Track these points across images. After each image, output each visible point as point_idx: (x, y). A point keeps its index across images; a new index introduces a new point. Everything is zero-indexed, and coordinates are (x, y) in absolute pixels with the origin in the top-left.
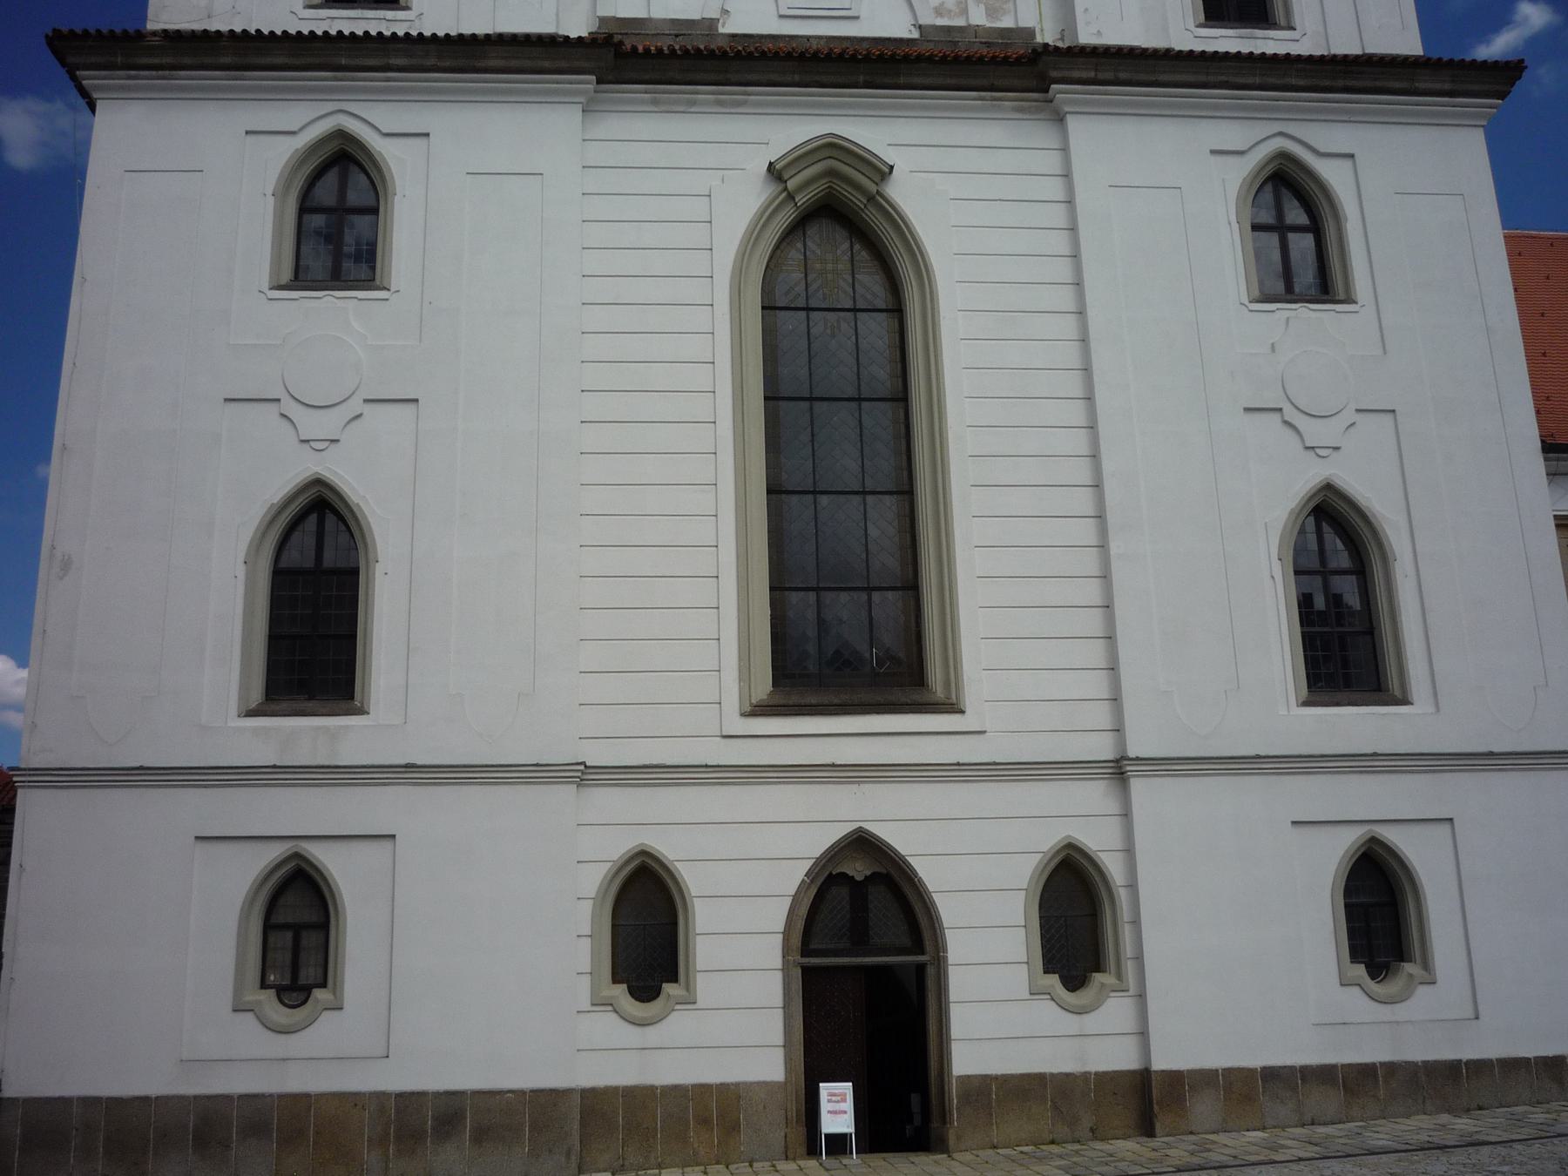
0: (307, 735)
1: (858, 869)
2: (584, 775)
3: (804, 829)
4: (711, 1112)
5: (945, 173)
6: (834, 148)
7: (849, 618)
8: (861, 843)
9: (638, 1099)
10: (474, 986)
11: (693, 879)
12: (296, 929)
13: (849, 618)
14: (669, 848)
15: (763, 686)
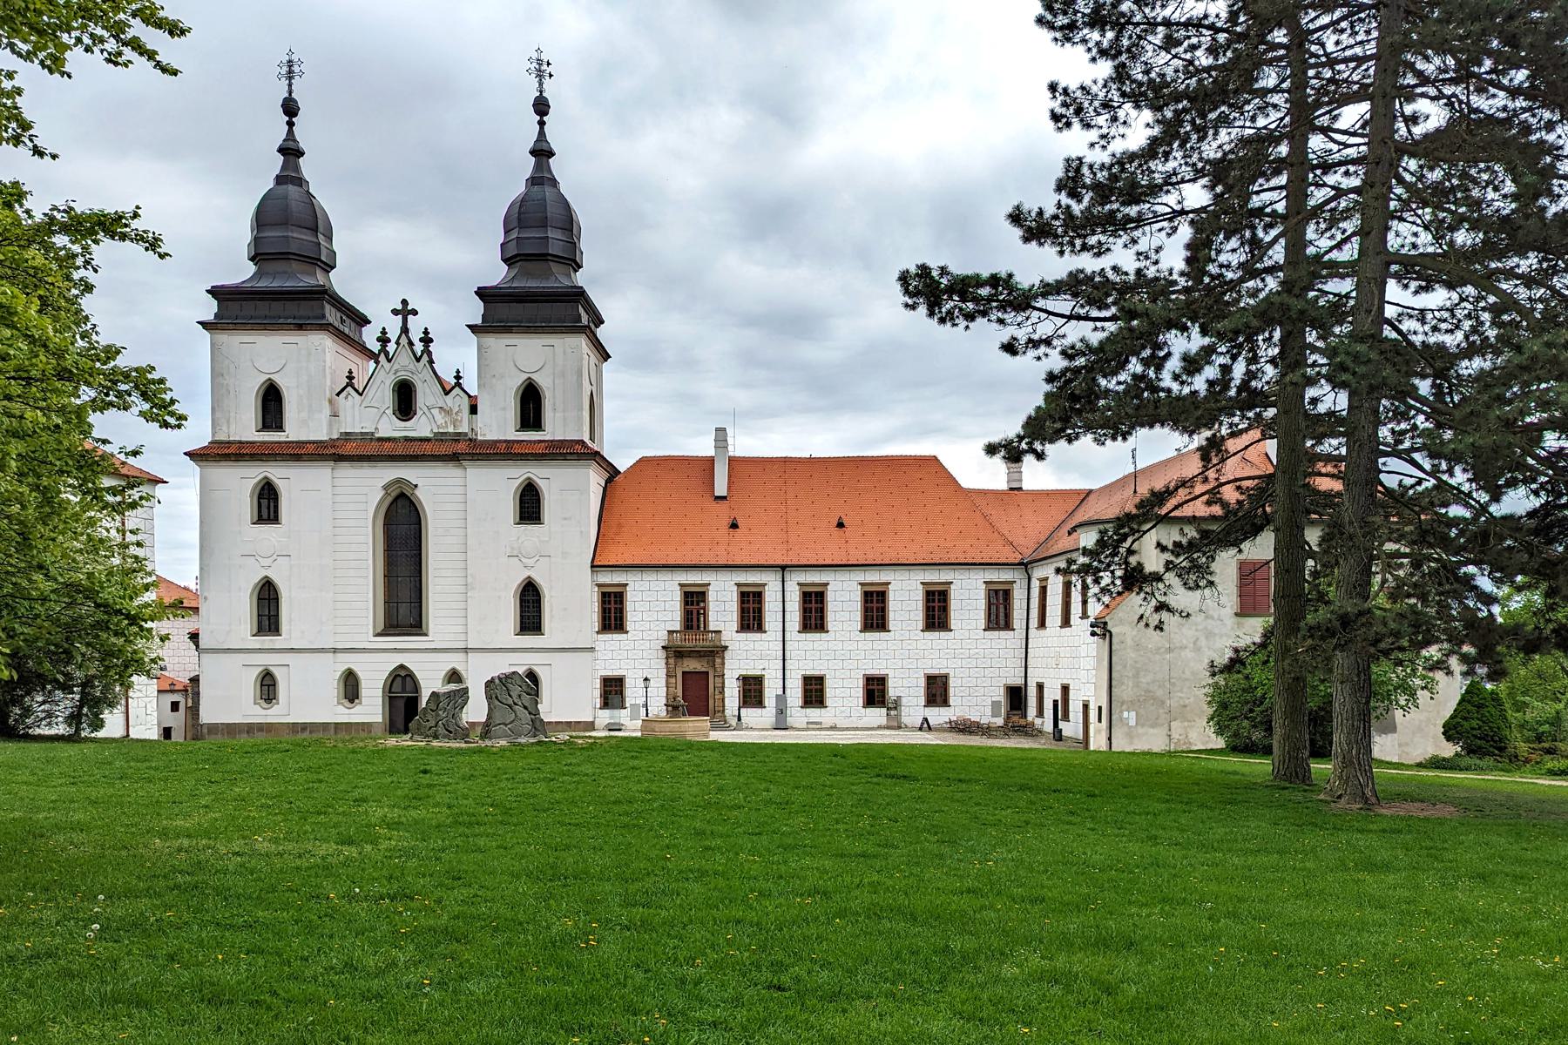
0: (268, 641)
1: (403, 673)
2: (335, 651)
3: (391, 662)
4: (366, 727)
5: (434, 487)
6: (399, 481)
7: (403, 610)
8: (402, 667)
9: (348, 725)
10: (309, 699)
11: (360, 674)
12: (268, 686)
13: (403, 610)
14: (355, 668)
15: (381, 627)
